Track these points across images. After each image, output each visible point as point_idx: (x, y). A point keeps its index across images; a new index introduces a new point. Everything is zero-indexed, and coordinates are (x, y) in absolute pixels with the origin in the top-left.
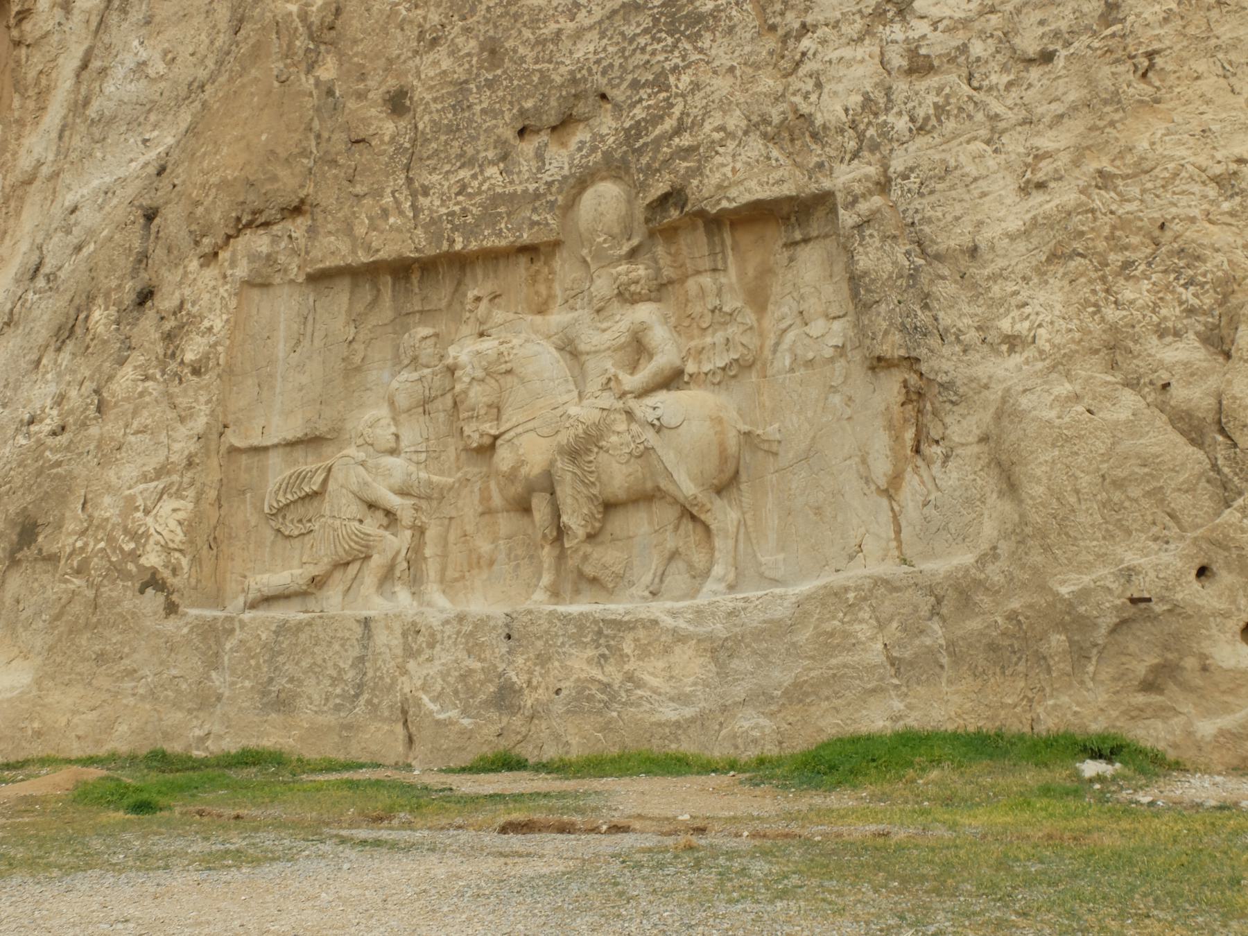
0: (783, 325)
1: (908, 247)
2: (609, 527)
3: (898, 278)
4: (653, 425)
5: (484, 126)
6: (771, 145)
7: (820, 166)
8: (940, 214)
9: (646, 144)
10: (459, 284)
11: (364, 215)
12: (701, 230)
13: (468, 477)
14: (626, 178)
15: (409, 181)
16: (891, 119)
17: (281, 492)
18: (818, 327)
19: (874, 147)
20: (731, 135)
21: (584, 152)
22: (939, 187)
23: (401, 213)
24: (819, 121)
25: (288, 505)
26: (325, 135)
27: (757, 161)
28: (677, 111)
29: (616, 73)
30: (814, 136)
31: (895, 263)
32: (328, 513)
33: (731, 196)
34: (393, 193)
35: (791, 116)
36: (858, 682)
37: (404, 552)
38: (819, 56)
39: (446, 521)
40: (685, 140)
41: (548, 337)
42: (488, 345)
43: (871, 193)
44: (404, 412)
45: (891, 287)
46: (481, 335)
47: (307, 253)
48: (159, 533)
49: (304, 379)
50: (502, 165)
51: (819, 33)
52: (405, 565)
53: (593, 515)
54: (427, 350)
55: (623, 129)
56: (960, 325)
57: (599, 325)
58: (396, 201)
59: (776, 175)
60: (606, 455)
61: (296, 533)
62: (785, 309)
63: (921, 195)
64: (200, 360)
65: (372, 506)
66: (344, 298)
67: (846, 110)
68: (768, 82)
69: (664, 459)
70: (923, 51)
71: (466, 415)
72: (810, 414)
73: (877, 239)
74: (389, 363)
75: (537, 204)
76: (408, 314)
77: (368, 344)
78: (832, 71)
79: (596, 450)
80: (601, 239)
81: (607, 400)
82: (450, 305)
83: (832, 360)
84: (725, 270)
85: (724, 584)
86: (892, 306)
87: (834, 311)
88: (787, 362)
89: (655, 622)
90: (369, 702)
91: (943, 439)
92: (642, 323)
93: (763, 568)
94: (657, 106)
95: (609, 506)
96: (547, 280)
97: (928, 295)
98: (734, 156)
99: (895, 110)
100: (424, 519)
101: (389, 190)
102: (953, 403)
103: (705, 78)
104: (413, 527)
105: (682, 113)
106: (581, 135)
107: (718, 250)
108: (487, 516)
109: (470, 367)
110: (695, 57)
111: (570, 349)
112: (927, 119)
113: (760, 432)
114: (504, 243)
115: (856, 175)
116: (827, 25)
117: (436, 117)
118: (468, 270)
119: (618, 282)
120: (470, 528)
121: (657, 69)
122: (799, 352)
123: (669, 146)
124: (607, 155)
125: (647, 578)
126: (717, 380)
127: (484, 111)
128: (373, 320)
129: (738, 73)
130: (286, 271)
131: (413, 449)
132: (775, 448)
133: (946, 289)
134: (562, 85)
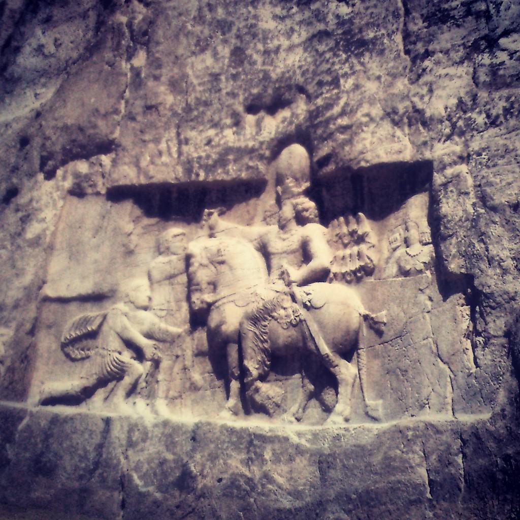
0: (394, 246)
1: (474, 201)
3: (466, 221)
4: (305, 306)
5: (227, 103)
6: (396, 128)
7: (425, 143)
8: (498, 181)
9: (321, 122)
15: (178, 134)
16: (474, 115)
18: (416, 248)
19: (462, 134)
20: (372, 120)
22: (500, 162)
23: (170, 154)
24: (428, 114)
26: (131, 101)
28: (342, 102)
29: (309, 75)
30: (425, 124)
31: (465, 211)
35: (411, 109)
38: (433, 72)
40: (344, 121)
41: (251, 241)
42: (213, 244)
43: (455, 163)
45: (460, 227)
50: (235, 129)
51: (435, 57)
53: (264, 362)
54: (176, 245)
56: (502, 255)
58: (169, 148)
59: (396, 146)
60: (276, 322)
62: (397, 235)
63: (488, 167)
65: (129, 344)
67: (446, 108)
68: (401, 85)
70: (501, 72)
73: (455, 194)
78: (441, 82)
79: (270, 318)
81: (280, 286)
83: (420, 272)
86: (460, 239)
91: (485, 331)
94: (330, 98)
97: (483, 234)
100: (160, 355)
101: (164, 140)
103: (362, 81)
104: (152, 360)
106: (285, 113)
110: (358, 67)
111: (264, 251)
112: (497, 117)
113: (373, 316)
115: (447, 151)
116: (441, 52)
117: (198, 95)
120: (188, 363)
121: (334, 74)
123: (334, 124)
124: (299, 127)
125: (294, 408)
127: (228, 94)
129: (383, 80)
131: (159, 308)
133: (496, 230)
134: (277, 80)
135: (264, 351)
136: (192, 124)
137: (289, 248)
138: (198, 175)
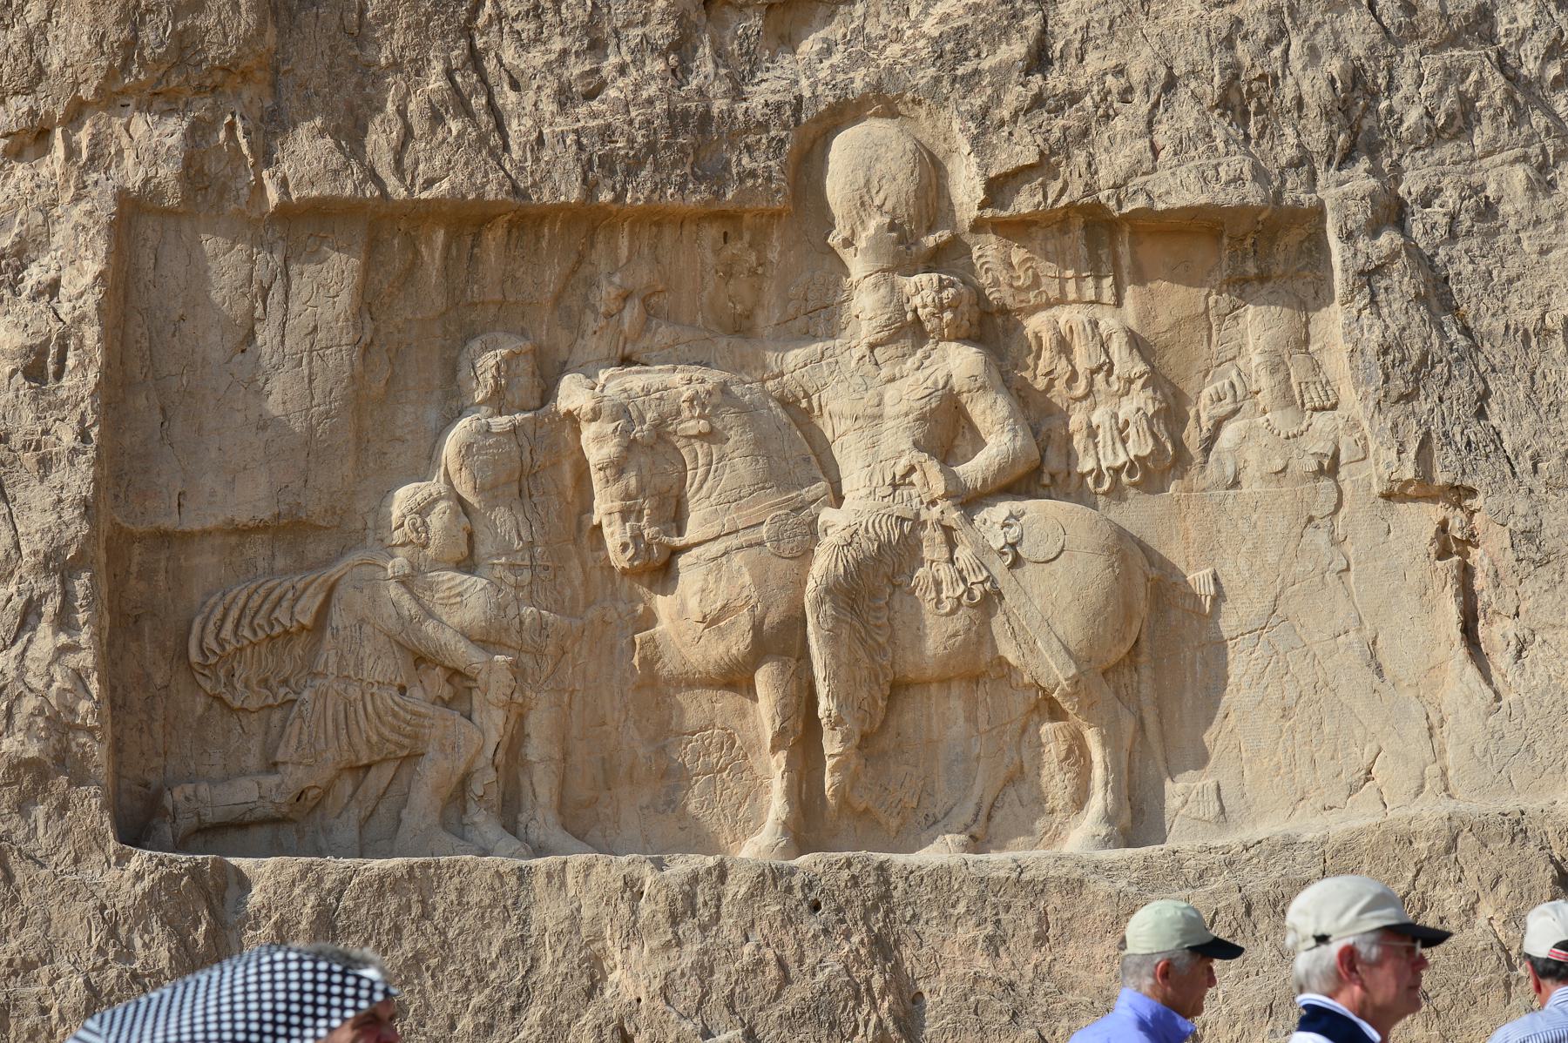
10: (581, 259)
11: (390, 108)
17: (229, 626)
21: (836, 58)
24: (1288, 92)
25: (241, 650)
32: (332, 668)
33: (1157, 191)
34: (449, 73)
36: (1457, 974)
37: (490, 754)
46: (626, 361)
48: (31, 690)
52: (491, 775)
53: (874, 698)
55: (923, 36)
61: (253, 703)
64: (40, 351)
71: (617, 504)
72: (1272, 557)
74: (438, 394)
75: (751, 139)
82: (558, 299)
84: (1119, 303)
87: (1314, 396)
88: (1230, 471)
89: (1081, 882)
90: (545, 1021)
92: (974, 377)
96: (753, 272)
98: (1150, 124)
99: (1400, 94)
100: (528, 693)
102: (1540, 564)
105: (1044, 31)
112: (1451, 117)
122: (1252, 455)
130: (223, 190)
136: (527, 27)
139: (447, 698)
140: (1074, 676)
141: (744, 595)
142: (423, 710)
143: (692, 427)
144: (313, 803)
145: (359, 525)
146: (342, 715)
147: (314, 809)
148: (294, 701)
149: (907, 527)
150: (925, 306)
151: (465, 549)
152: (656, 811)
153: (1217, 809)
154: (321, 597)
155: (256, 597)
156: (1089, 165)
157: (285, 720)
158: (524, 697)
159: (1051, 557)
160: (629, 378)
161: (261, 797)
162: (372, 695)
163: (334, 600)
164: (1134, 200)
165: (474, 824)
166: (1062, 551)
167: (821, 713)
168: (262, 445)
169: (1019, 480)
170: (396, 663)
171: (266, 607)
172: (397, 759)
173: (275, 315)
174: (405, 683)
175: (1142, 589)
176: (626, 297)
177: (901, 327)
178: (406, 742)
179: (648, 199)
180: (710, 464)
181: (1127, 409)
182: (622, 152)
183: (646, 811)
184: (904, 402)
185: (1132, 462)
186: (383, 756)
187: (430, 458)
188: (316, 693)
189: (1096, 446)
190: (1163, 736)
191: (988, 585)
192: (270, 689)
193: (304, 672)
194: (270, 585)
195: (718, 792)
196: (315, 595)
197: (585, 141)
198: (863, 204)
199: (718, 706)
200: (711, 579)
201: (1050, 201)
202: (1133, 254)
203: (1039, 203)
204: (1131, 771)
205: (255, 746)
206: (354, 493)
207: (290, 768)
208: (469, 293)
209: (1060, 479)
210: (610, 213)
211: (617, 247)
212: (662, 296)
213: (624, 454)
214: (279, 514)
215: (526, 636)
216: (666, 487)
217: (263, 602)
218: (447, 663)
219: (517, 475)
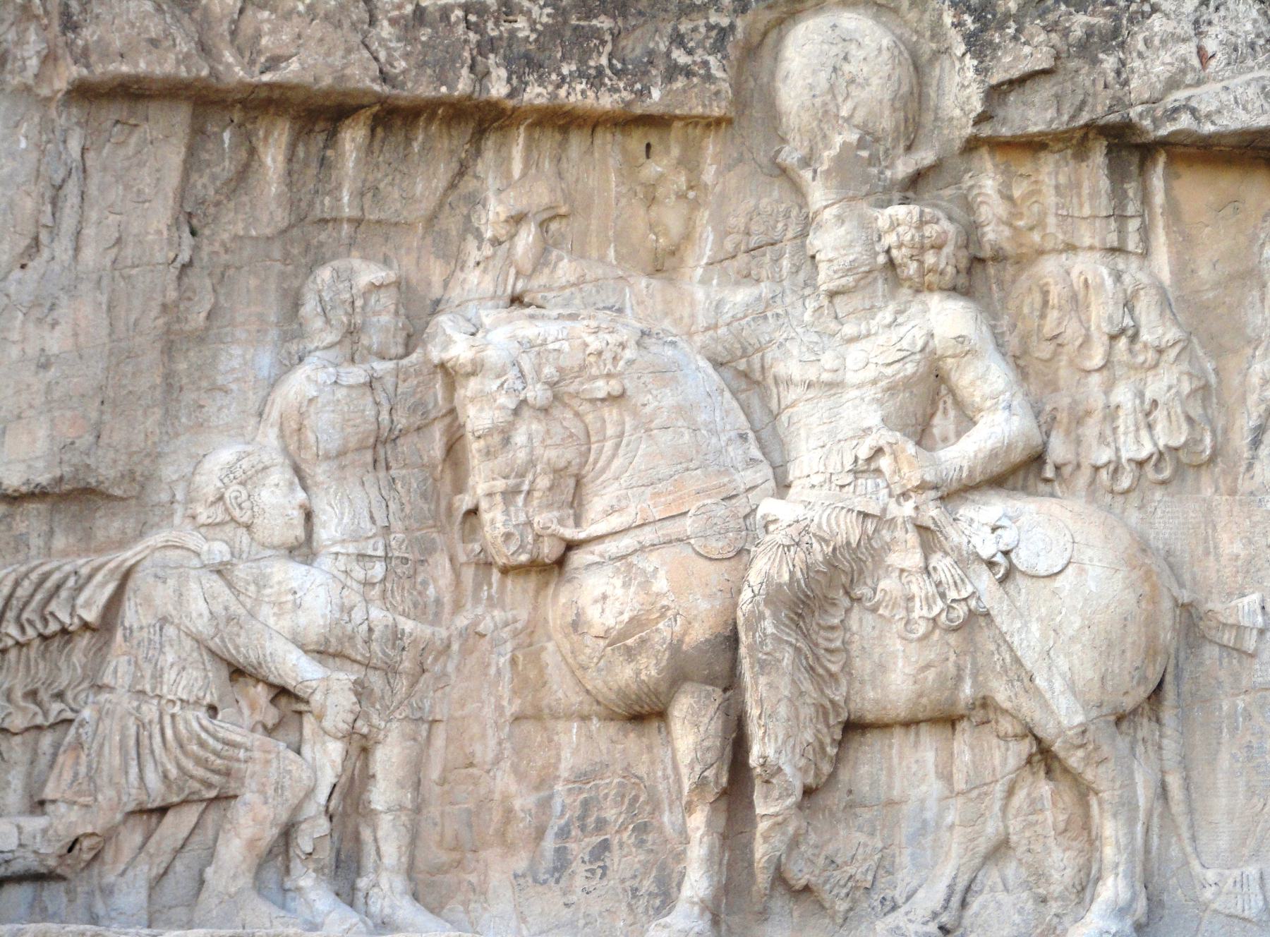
2: (844, 775)
4: (991, 564)
10: (462, 170)
12: (1098, 157)
13: (481, 628)
14: (912, 16)
27: (1252, 46)
33: (1204, 109)
39: (426, 726)
44: (327, 457)
46: (516, 300)
47: (75, 27)
49: (55, 342)
52: (323, 826)
53: (822, 746)
57: (833, 325)
60: (869, 618)
66: (174, 156)
69: (1016, 641)
71: (500, 484)
74: (273, 333)
76: (325, 221)
77: (222, 278)
79: (846, 602)
80: (854, 137)
82: (432, 219)
84: (1146, 254)
85: (1129, 922)
92: (960, 339)
93: (1208, 894)
95: (854, 728)
98: (1196, 23)
100: (375, 720)
107: (1131, 209)
108: (528, 727)
109: (512, 373)
114: (607, 102)
118: (490, 143)
119: (890, 239)
120: (485, 751)
126: (1125, 482)
128: (232, 224)
131: (352, 549)
132: (1250, 643)
135: (822, 712)
137: (889, 371)
138: (482, 76)
139: (270, 724)
140: (1081, 724)
141: (659, 606)
142: (238, 739)
143: (599, 389)
144: (87, 856)
145: (164, 497)
146: (132, 742)
147: (89, 864)
148: (70, 721)
149: (870, 526)
150: (900, 246)
151: (300, 532)
152: (535, 881)
153: (1261, 904)
154: (110, 588)
155: (26, 583)
156: (1118, 73)
157: (57, 746)
158: (371, 726)
159: (1056, 570)
160: (520, 323)
161: (21, 845)
162: (173, 716)
163: (129, 593)
164: (1175, 119)
165: (299, 889)
166: (1069, 563)
167: (754, 760)
168: (43, 387)
169: (1014, 470)
170: (206, 677)
171: (39, 597)
172: (202, 801)
173: (68, 222)
174: (216, 703)
175: (1170, 615)
176: (517, 220)
177: (870, 272)
178: (215, 779)
179: (554, 96)
180: (621, 435)
181: (1156, 387)
182: (521, 35)
183: (521, 881)
184: (871, 366)
185: (1161, 454)
186: (182, 797)
187: (260, 415)
188: (100, 711)
189: (1115, 430)
190: (1191, 811)
191: (973, 603)
192: (39, 704)
193: (85, 685)
194: (46, 568)
195: (616, 860)
196: (103, 585)
197: (473, 18)
198: (826, 112)
199: (620, 747)
200: (618, 582)
201: (1065, 118)
202: (1168, 191)
203: (1052, 121)
204: (1147, 851)
205: (16, 779)
206: (159, 455)
207: (62, 808)
208: (318, 206)
209: (1067, 471)
210: (503, 111)
211: (508, 160)
212: (564, 221)
213: (511, 418)
214: (61, 478)
215: (375, 647)
216: (562, 464)
217: (35, 590)
218: (272, 679)
219: (372, 440)
